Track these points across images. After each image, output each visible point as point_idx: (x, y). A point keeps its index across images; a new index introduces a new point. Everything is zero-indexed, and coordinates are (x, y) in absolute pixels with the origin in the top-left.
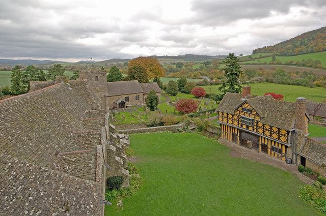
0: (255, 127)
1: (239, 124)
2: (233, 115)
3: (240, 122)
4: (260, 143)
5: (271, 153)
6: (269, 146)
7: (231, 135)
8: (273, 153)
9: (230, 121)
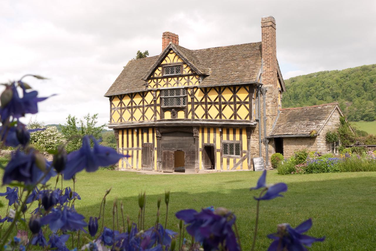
0: (190, 107)
1: (155, 111)
2: (143, 94)
4: (200, 146)
5: (222, 161)
6: (218, 146)
7: (140, 152)
8: (225, 160)
9: (138, 114)
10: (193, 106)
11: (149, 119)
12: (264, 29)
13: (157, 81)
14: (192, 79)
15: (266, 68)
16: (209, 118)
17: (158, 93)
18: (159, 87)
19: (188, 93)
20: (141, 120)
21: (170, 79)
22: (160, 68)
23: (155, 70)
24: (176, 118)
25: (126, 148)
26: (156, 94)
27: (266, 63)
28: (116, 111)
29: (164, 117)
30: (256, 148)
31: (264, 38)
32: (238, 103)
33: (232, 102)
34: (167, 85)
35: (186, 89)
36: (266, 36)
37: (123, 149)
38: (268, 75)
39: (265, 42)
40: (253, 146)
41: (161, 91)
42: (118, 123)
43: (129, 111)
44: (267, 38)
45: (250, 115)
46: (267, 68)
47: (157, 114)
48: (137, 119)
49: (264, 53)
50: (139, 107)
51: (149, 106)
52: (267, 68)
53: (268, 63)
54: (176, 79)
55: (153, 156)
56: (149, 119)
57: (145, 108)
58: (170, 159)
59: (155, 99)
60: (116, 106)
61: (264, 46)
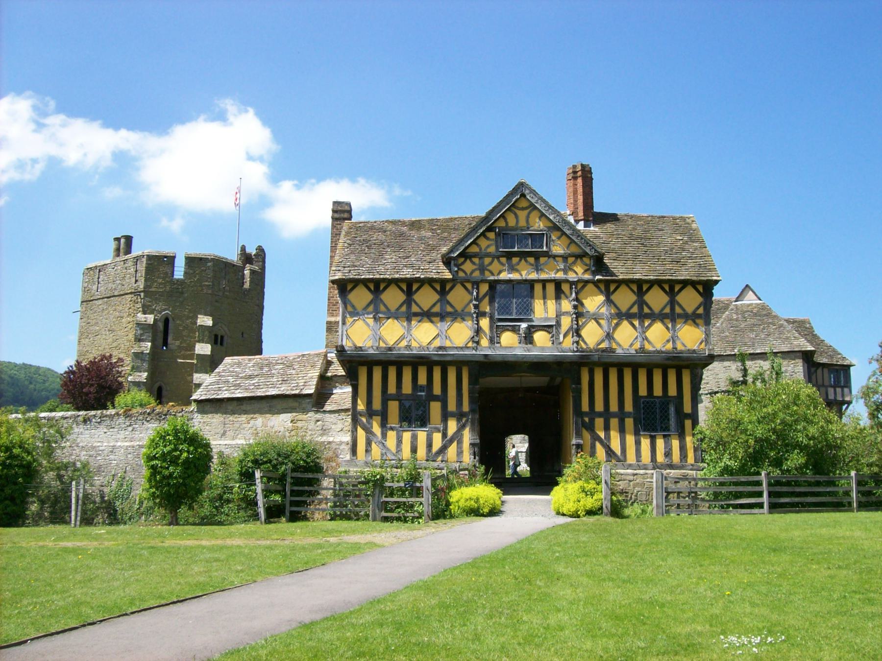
0: (566, 322)
17: (484, 288)
22: (491, 235)
26: (478, 289)
33: (666, 314)
54: (531, 260)
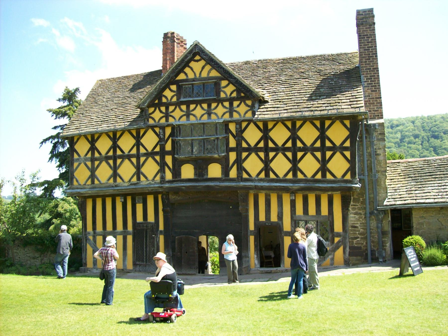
0: (233, 156)
1: (162, 165)
3: (169, 159)
4: (252, 227)
7: (130, 238)
10: (239, 156)
11: (150, 177)
12: (363, 29)
13: (167, 109)
14: (238, 106)
15: (370, 92)
16: (272, 176)
17: (168, 131)
18: (171, 120)
19: (228, 130)
20: (134, 180)
21: (194, 106)
22: (174, 87)
23: (164, 89)
24: (205, 177)
25: (101, 232)
27: (370, 84)
28: (82, 165)
29: (180, 174)
30: (359, 227)
31: (362, 43)
32: (329, 149)
34: (187, 117)
35: (226, 124)
36: (367, 40)
37: (95, 233)
38: (374, 103)
39: (366, 50)
40: (354, 224)
41: (173, 127)
42: (86, 187)
43: (109, 164)
44: (368, 42)
45: (352, 170)
46: (372, 91)
47: (167, 170)
48: (126, 179)
49: (365, 67)
50: (129, 157)
51: (151, 154)
52: (372, 91)
53: (373, 83)
54: (205, 106)
55: (156, 246)
56: (150, 177)
57: (142, 159)
58: (191, 251)
59: (163, 143)
60: (82, 154)
61: (365, 55)
